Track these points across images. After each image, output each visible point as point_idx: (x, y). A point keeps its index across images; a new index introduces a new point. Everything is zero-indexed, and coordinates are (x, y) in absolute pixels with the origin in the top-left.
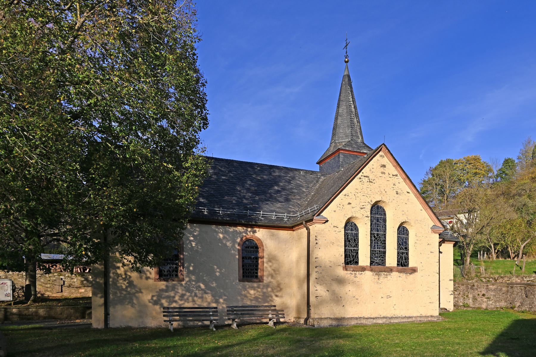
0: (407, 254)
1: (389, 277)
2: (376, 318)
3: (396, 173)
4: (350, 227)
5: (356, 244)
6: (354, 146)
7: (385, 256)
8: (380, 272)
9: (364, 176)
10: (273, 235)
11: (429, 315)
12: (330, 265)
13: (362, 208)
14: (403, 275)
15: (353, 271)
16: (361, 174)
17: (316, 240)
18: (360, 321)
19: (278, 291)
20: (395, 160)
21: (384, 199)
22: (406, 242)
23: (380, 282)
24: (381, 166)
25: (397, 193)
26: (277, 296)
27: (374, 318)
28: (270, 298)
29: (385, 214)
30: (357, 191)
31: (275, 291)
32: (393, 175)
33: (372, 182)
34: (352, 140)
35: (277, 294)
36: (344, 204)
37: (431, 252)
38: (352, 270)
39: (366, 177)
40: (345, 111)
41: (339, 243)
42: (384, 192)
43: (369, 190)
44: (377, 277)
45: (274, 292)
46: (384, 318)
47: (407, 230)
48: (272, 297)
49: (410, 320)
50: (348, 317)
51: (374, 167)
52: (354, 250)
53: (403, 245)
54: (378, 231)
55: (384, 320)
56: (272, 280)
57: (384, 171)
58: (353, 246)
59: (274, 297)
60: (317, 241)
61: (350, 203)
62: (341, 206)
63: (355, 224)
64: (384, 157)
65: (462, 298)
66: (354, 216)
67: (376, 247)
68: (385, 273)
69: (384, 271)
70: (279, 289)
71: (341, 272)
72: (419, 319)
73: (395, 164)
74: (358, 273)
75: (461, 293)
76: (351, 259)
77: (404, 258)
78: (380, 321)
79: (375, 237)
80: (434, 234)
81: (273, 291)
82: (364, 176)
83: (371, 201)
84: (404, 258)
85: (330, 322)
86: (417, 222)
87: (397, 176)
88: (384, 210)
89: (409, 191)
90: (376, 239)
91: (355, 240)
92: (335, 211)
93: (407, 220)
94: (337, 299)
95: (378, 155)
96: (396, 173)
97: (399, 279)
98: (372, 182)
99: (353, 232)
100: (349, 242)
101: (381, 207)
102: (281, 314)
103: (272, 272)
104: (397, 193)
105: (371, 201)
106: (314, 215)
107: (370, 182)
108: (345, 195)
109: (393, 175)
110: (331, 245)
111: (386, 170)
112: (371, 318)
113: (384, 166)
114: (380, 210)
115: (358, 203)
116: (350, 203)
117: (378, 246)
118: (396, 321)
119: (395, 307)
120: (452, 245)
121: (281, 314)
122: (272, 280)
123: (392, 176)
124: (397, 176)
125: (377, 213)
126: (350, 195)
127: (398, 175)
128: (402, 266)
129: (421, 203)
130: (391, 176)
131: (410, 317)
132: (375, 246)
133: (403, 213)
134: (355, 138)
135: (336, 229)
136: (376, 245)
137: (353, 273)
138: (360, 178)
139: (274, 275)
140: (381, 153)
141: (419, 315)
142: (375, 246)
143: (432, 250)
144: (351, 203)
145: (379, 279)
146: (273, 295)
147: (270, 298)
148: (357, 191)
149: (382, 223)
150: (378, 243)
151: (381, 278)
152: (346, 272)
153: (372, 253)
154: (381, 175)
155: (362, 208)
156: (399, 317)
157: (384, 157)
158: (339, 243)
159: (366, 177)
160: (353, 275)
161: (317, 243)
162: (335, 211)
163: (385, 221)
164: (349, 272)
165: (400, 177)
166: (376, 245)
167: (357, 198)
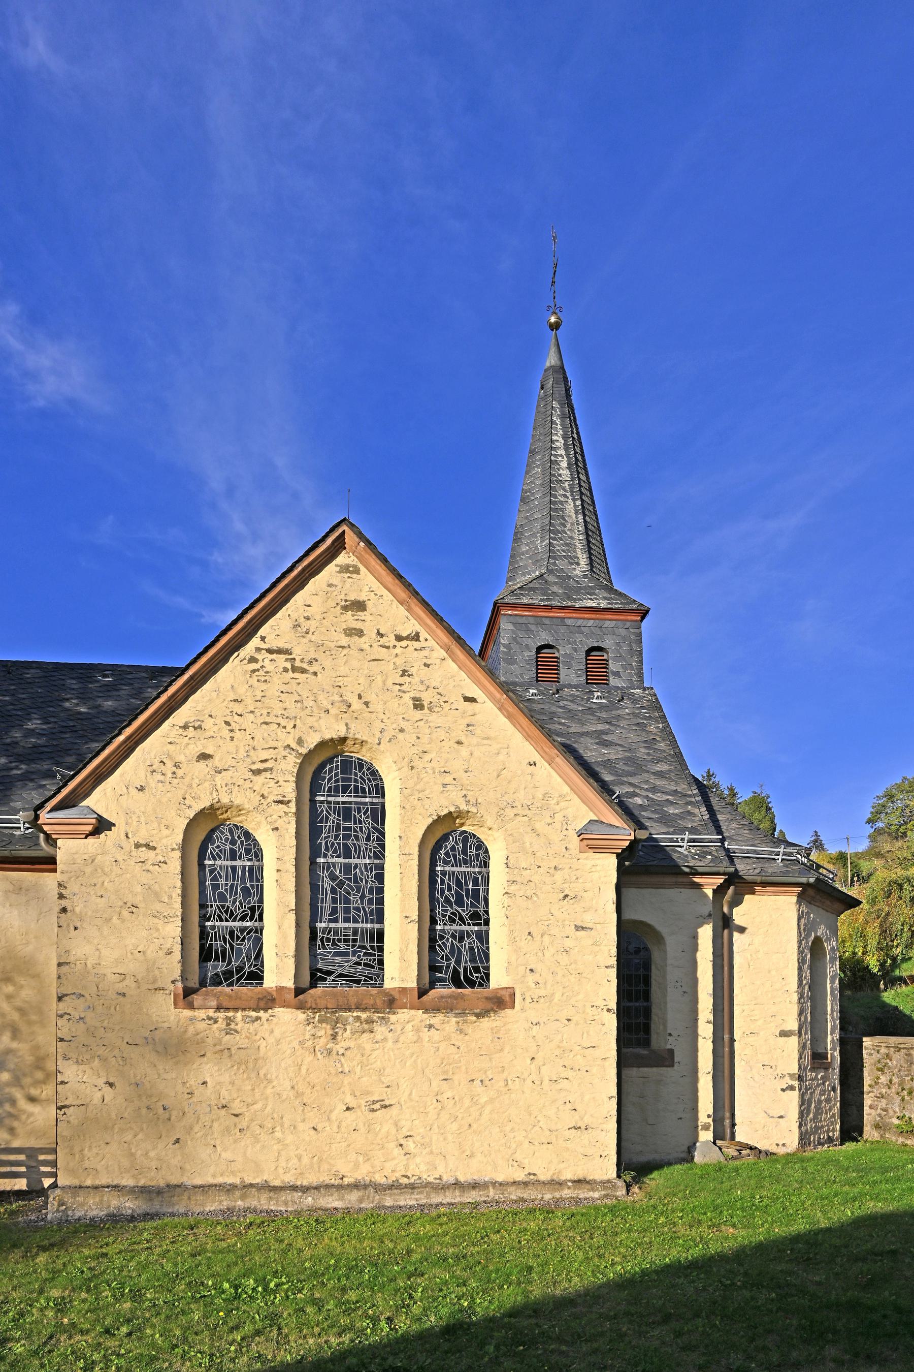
0: (483, 938)
1: (380, 1030)
2: (317, 1188)
3: (410, 626)
4: (215, 841)
5: (253, 909)
6: (555, 589)
7: (381, 949)
8: (339, 1008)
9: (270, 651)
10: (19, 889)
11: (568, 1175)
12: (120, 987)
13: (257, 772)
14: (448, 1023)
15: (218, 1009)
16: (255, 642)
17: (61, 896)
18: (243, 1197)
19: (36, 1083)
20: (400, 577)
21: (358, 731)
22: (476, 893)
23: (339, 1048)
24: (345, 608)
25: (418, 705)
26: (32, 1099)
27: (305, 1189)
28: (7, 1107)
29: (380, 791)
30: (238, 708)
31: (27, 1081)
32: (399, 638)
33: (304, 671)
34: (550, 571)
35: (34, 1092)
36: (181, 758)
37: (579, 928)
38: (214, 1003)
39: (279, 651)
40: (538, 482)
41: (158, 906)
42: (357, 705)
43: (289, 701)
44: (325, 1030)
45: (22, 1087)
46: (356, 1186)
47: (480, 846)
48: (13, 1102)
49: (472, 1196)
50: (198, 1181)
51: (314, 611)
52: (242, 930)
53: (460, 902)
54: (348, 855)
55: (353, 1197)
56: (14, 1045)
57: (358, 625)
58: (239, 913)
59: (23, 1104)
60: (64, 903)
61: (204, 757)
62: (169, 768)
63: (247, 835)
64: (357, 571)
65: (898, 1100)
66: (225, 800)
67: (340, 914)
68: (364, 1015)
69: (358, 1008)
70: (39, 1075)
71: (167, 1012)
72: (515, 1194)
73: (403, 594)
74: (239, 1015)
75: (895, 1080)
76: (219, 960)
77: (466, 956)
78: (333, 1202)
79: (333, 877)
80: (590, 854)
81: (17, 1081)
82: (270, 651)
83: (300, 742)
84: (466, 956)
85: (115, 1203)
86: (510, 812)
87: (416, 637)
88: (374, 773)
89: (474, 691)
90: (341, 884)
91: (246, 892)
92: (141, 789)
93: (463, 807)
94: (159, 1116)
95: (331, 568)
96: (410, 626)
97: (426, 1034)
98: (304, 671)
99: (238, 863)
100: (222, 897)
101: (361, 764)
102: (45, 1163)
103: (15, 1016)
104: (418, 705)
105: (300, 742)
106: (41, 806)
107: (294, 669)
108: (185, 727)
109: (399, 638)
110: (125, 913)
111: (368, 622)
112: (294, 1188)
113: (359, 606)
114: (356, 774)
115: (242, 753)
116: (204, 757)
117: (347, 910)
118: (407, 1200)
119: (410, 1145)
120: (795, 899)
121: (45, 1163)
122: (14, 1045)
123: (393, 641)
124: (416, 637)
125: (345, 789)
126: (208, 723)
127: (423, 635)
128: (458, 985)
129: (528, 737)
130: (390, 640)
131: (475, 1186)
132: (334, 911)
133: (448, 779)
134: (561, 564)
135: (144, 853)
136: (340, 907)
137: (221, 1015)
138: (253, 660)
139: (23, 1028)
140: (342, 559)
141: (520, 1176)
142: (334, 911)
143: (588, 919)
144: (215, 753)
145: (334, 1037)
146: (18, 1095)
147: (7, 1107)
148: (238, 708)
149: (368, 824)
150: (347, 901)
151: (346, 1039)
152: (187, 1013)
153: (431, 941)
154: (344, 641)
155: (257, 772)
156: (428, 1184)
157: (357, 571)
158: (158, 906)
159: (279, 651)
160: (221, 1024)
161: (64, 910)
162: (141, 789)
163: (379, 814)
164: (201, 1014)
165: (432, 643)
166: (340, 907)
167: (238, 735)
